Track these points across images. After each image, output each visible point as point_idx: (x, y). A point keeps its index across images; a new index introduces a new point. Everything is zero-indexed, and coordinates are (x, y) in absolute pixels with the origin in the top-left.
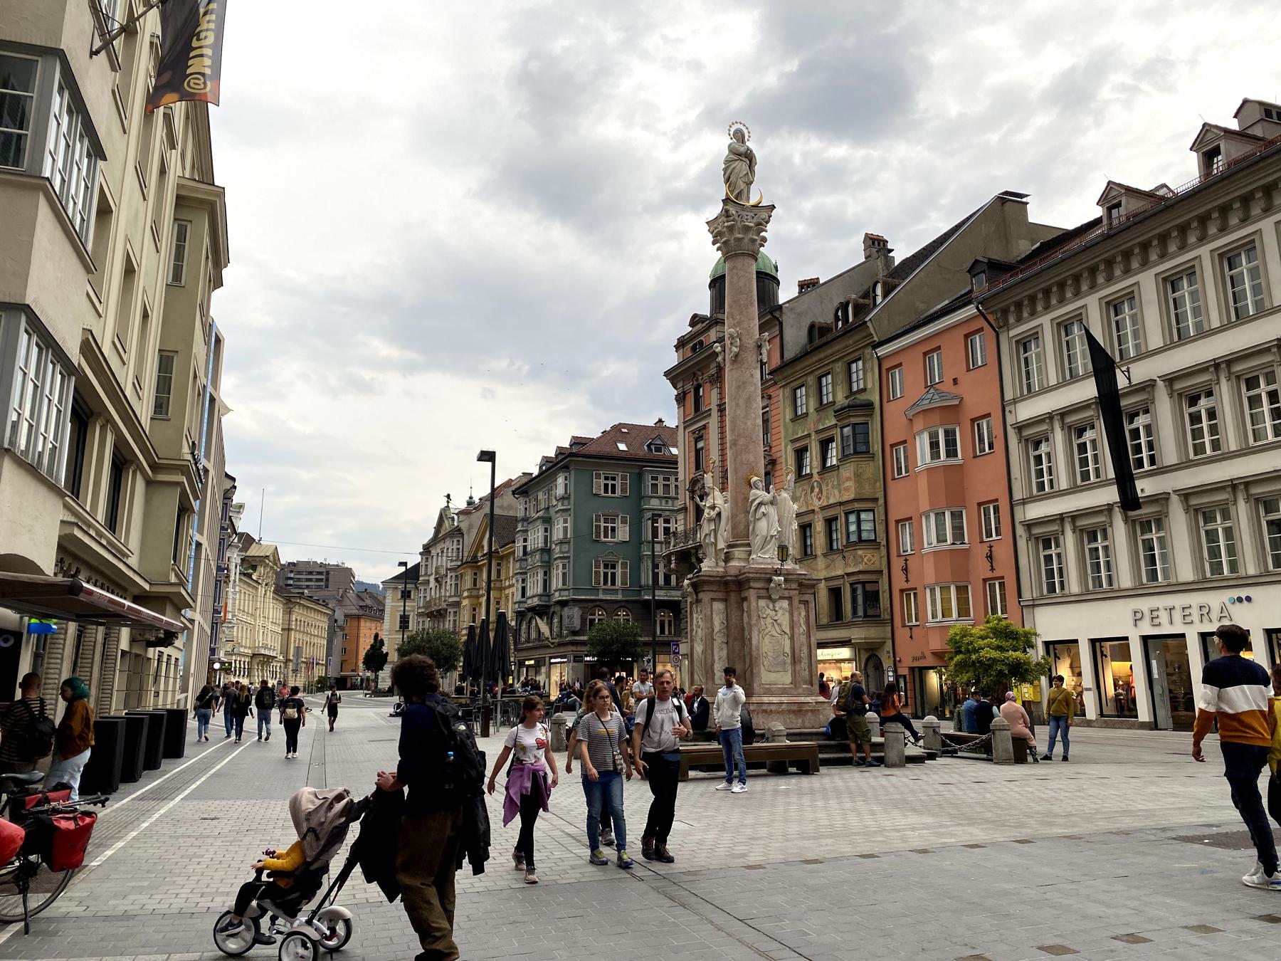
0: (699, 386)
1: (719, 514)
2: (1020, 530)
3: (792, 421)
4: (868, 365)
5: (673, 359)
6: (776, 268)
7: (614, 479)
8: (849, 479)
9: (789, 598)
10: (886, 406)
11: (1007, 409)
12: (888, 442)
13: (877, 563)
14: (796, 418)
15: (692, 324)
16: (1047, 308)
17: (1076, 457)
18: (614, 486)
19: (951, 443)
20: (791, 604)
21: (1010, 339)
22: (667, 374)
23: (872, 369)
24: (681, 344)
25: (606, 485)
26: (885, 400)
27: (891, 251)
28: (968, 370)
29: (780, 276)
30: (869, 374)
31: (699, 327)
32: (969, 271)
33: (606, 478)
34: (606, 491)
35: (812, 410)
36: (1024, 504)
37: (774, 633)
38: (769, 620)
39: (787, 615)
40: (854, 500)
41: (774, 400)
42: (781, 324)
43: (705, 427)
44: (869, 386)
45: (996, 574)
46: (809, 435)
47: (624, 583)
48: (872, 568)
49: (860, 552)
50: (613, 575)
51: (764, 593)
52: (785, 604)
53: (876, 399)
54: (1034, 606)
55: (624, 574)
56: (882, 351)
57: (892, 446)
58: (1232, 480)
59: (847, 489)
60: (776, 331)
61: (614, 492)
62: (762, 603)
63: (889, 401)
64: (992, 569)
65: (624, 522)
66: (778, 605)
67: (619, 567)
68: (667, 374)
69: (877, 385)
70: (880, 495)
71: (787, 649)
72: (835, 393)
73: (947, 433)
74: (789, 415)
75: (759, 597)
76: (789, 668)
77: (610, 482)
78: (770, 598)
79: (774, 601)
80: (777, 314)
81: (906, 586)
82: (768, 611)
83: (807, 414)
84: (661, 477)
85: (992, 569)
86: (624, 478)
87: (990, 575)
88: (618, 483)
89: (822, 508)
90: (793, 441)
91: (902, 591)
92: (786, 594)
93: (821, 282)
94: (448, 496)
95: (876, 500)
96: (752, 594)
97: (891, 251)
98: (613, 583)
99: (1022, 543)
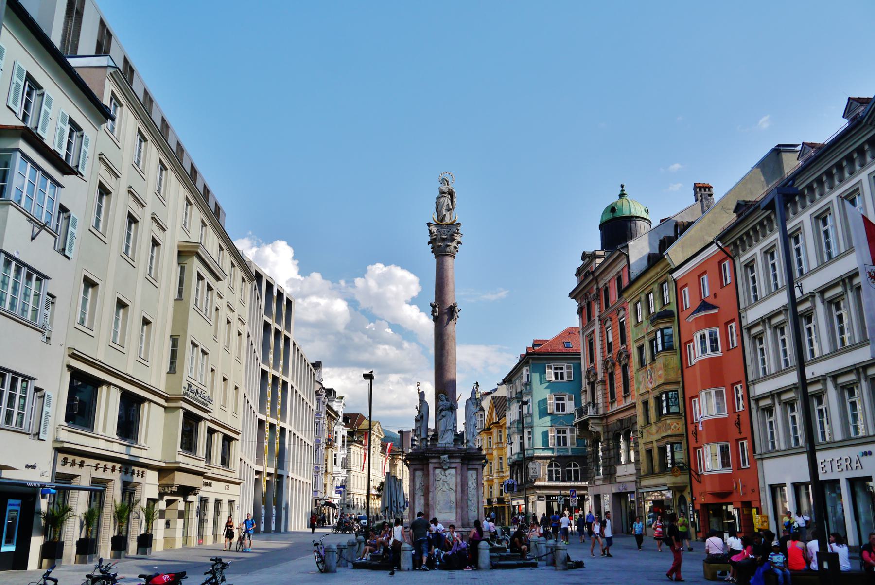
3: (636, 326)
4: (670, 286)
7: (562, 369)
8: (660, 369)
9: (455, 468)
10: (681, 314)
12: (684, 340)
13: (681, 429)
14: (638, 324)
15: (583, 259)
18: (562, 374)
19: (714, 341)
21: (741, 264)
24: (579, 273)
25: (556, 374)
28: (722, 287)
31: (587, 260)
33: (556, 369)
34: (556, 378)
36: (754, 384)
37: (444, 489)
38: (441, 481)
39: (454, 478)
40: (664, 384)
43: (593, 332)
47: (572, 443)
48: (677, 433)
49: (668, 422)
50: (565, 438)
51: (436, 465)
52: (453, 471)
53: (673, 307)
54: (762, 459)
55: (572, 437)
56: (675, 275)
58: (854, 365)
59: (660, 376)
61: (562, 378)
62: (438, 471)
63: (683, 310)
64: (740, 433)
65: (570, 399)
66: (447, 472)
67: (568, 431)
68: (570, 295)
70: (680, 380)
71: (453, 499)
72: (655, 307)
74: (633, 322)
75: (435, 468)
76: (454, 510)
77: (559, 371)
78: (442, 468)
79: (445, 470)
80: (624, 251)
81: (696, 445)
82: (441, 476)
85: (740, 433)
87: (739, 436)
88: (565, 372)
89: (653, 389)
91: (695, 449)
92: (453, 465)
94: (477, 383)
95: (678, 383)
96: (431, 466)
98: (565, 444)
99: (754, 412)
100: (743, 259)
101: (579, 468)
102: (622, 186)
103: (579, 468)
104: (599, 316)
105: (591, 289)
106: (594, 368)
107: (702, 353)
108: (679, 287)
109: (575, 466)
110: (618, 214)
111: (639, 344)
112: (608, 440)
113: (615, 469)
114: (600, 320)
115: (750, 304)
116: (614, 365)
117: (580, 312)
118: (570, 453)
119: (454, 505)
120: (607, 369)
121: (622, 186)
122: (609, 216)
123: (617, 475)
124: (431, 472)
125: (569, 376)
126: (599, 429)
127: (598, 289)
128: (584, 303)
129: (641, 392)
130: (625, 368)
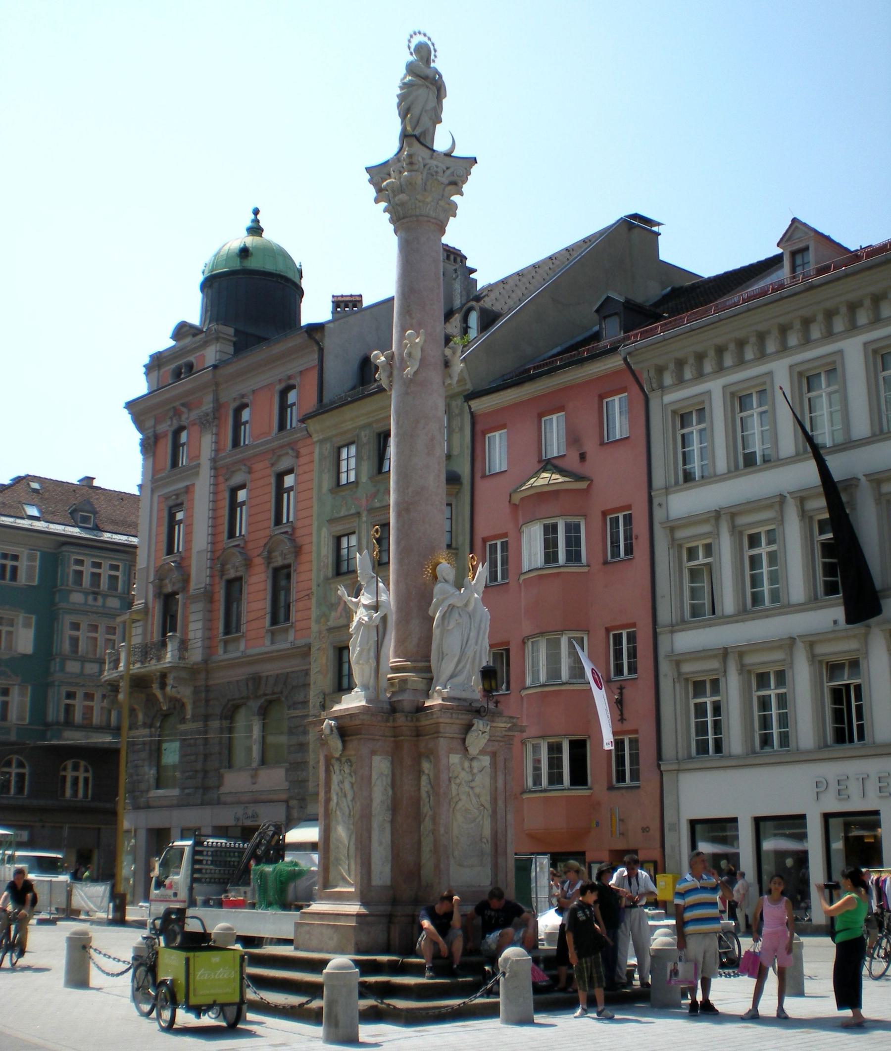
0: (181, 429)
1: (384, 619)
2: (665, 667)
3: (331, 491)
5: (140, 387)
6: (300, 273)
11: (656, 502)
16: (720, 369)
17: (748, 572)
18: (15, 569)
19: (573, 542)
20: (494, 764)
22: (130, 405)
23: (461, 429)
24: (156, 363)
26: (478, 475)
27: (473, 271)
29: (304, 284)
30: (456, 437)
31: (188, 340)
32: (597, 311)
35: (364, 479)
41: (302, 460)
42: (321, 350)
43: (188, 490)
44: (456, 451)
45: (627, 726)
46: (358, 514)
56: (475, 404)
57: (485, 540)
60: (313, 359)
61: (14, 577)
65: (27, 625)
66: (475, 764)
68: (130, 405)
69: (467, 452)
71: (487, 832)
73: (569, 528)
74: (327, 483)
80: (318, 336)
83: (356, 483)
84: (106, 564)
86: (31, 558)
88: (23, 565)
90: (331, 521)
93: (366, 303)
97: (473, 271)
99: (666, 685)
100: (668, 398)
101: (26, 771)
102: (256, 212)
103: (26, 771)
104: (214, 460)
105: (176, 401)
106: (182, 567)
107: (547, 561)
108: (479, 428)
109: (21, 765)
110: (253, 264)
111: (339, 529)
112: (206, 718)
113: (221, 778)
114: (214, 468)
115: (677, 483)
116: (248, 563)
117: (149, 447)
118: (13, 737)
119: (488, 848)
120: (223, 572)
121: (256, 212)
122: (237, 265)
123: (223, 790)
124: (444, 761)
125: (30, 577)
126: (185, 693)
127: (218, 407)
128: (166, 427)
129: (331, 624)
130: (281, 576)
